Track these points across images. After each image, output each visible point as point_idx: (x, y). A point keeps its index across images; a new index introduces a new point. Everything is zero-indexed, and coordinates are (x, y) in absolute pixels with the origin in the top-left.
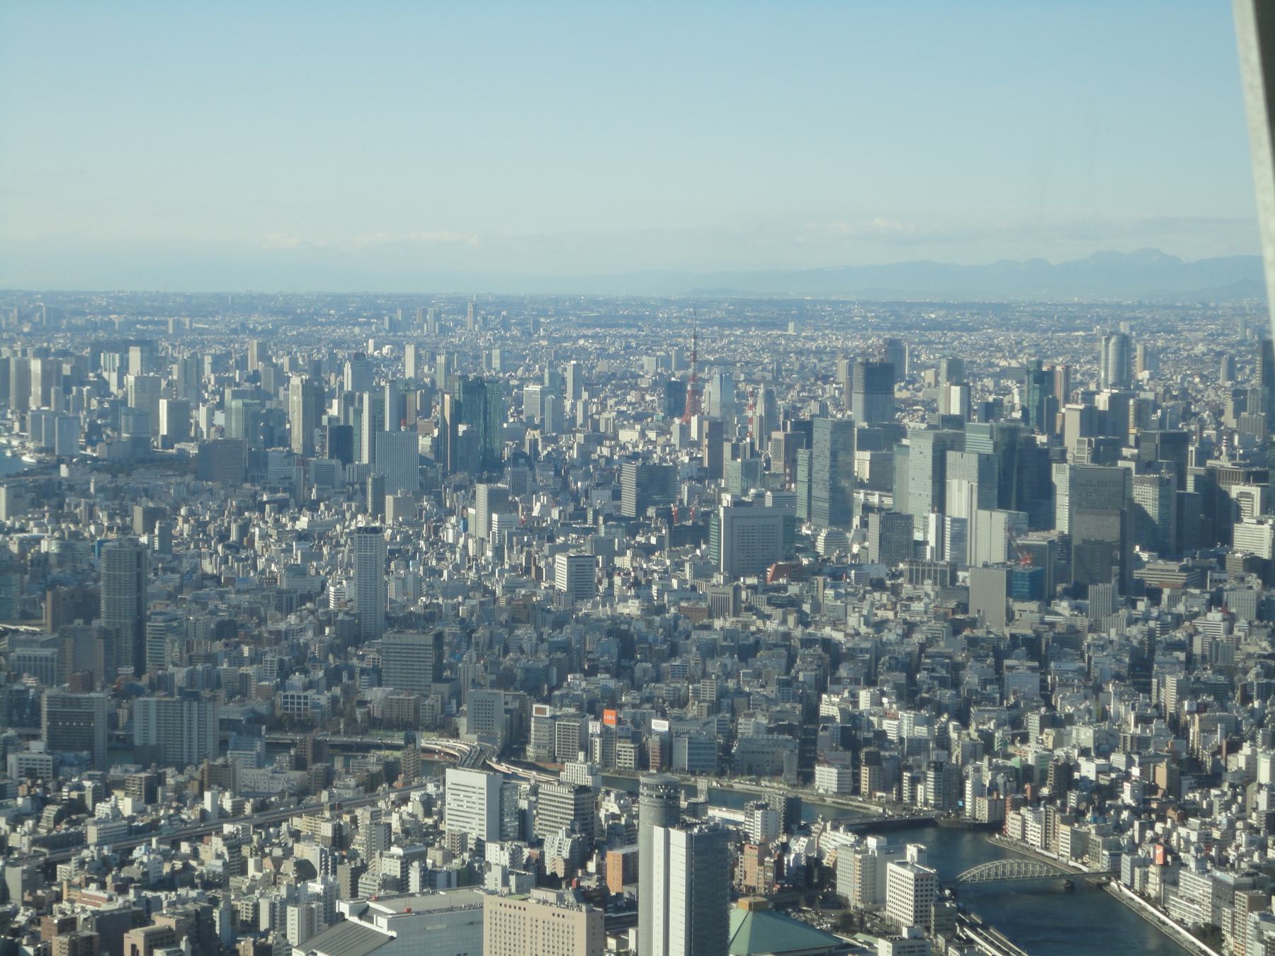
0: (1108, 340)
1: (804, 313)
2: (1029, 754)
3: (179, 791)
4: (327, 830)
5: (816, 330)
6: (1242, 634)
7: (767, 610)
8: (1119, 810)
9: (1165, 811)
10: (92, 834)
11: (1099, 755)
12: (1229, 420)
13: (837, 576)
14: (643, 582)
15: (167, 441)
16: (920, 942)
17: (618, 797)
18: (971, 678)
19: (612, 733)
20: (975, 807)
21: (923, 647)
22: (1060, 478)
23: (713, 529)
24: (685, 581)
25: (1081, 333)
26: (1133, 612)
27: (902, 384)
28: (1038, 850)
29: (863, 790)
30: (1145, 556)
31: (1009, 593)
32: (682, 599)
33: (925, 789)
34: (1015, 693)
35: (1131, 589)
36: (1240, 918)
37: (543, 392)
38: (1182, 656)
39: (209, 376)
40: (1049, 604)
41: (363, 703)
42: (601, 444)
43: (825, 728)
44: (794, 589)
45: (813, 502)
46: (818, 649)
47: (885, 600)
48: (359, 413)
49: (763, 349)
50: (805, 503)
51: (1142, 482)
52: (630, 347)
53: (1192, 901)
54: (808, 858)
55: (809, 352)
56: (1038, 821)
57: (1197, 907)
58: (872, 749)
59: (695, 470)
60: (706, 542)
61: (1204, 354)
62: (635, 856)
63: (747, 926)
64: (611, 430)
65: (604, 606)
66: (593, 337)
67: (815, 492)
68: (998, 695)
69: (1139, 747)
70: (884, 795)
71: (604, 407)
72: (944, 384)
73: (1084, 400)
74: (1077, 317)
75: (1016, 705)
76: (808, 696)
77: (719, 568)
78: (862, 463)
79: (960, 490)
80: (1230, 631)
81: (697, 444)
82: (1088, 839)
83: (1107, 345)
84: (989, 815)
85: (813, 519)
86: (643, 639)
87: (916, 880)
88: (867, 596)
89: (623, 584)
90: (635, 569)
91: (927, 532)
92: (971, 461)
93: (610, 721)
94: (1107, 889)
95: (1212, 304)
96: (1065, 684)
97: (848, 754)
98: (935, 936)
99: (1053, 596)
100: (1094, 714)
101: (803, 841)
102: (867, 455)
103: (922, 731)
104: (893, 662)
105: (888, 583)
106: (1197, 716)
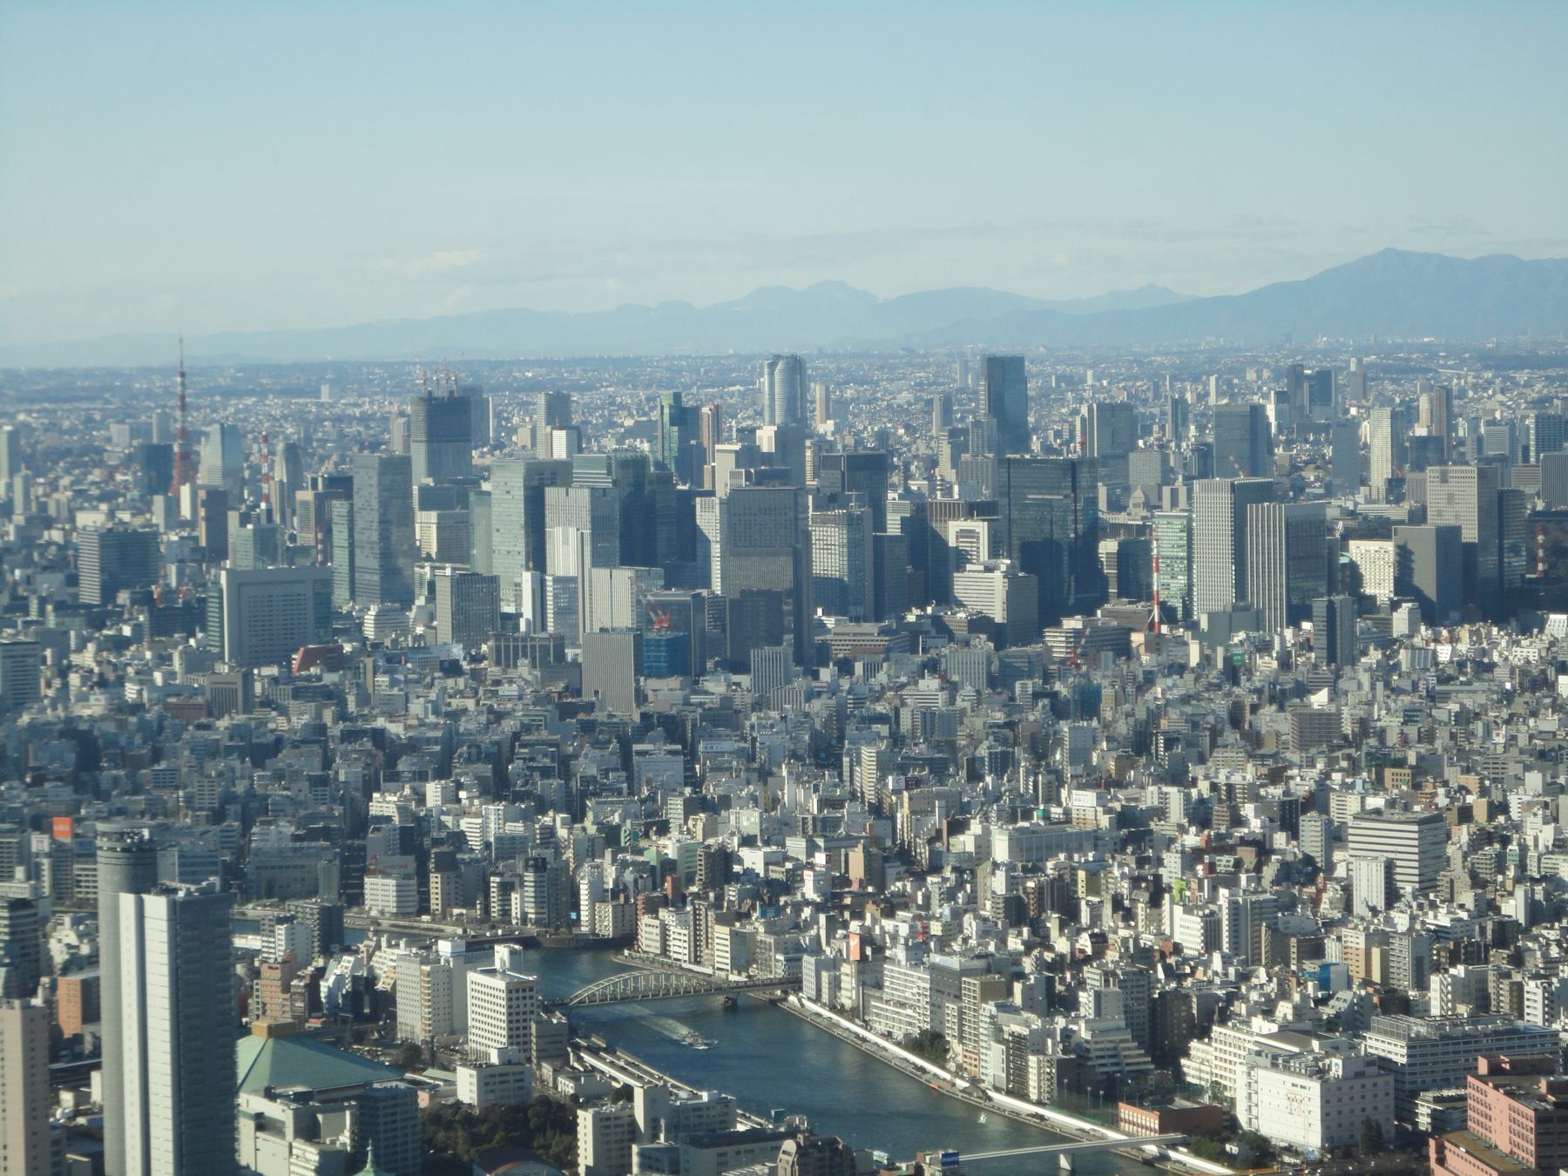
0: (772, 366)
1: (345, 377)
2: (669, 846)
5: (360, 396)
6: (967, 705)
7: (293, 704)
8: (798, 908)
9: (863, 906)
11: (767, 843)
12: (945, 470)
13: (392, 661)
14: (111, 677)
16: (517, 1069)
17: (76, 922)
18: (586, 766)
19: (65, 851)
20: (594, 918)
21: (516, 736)
22: (709, 519)
23: (212, 606)
24: (173, 674)
25: (738, 387)
26: (814, 684)
27: (485, 450)
28: (685, 966)
29: (433, 907)
30: (830, 622)
31: (639, 670)
32: (169, 696)
33: (522, 897)
34: (649, 783)
35: (811, 656)
36: (970, 1015)
38: (884, 730)
40: (697, 682)
42: (49, 527)
43: (378, 830)
44: (330, 678)
45: (357, 575)
46: (368, 744)
47: (462, 687)
49: (285, 417)
50: (346, 578)
51: (824, 522)
52: (94, 421)
53: (903, 1005)
54: (356, 980)
55: (351, 419)
56: (683, 924)
57: (909, 1012)
58: (445, 849)
59: (186, 551)
60: (202, 630)
61: (910, 404)
62: (98, 979)
63: (266, 1059)
64: (65, 514)
65: (55, 708)
66: (38, 411)
67: (360, 561)
68: (625, 785)
69: (824, 829)
70: (464, 911)
71: (54, 486)
72: (544, 429)
73: (740, 440)
74: (733, 370)
75: (652, 798)
76: (352, 799)
77: (222, 658)
78: (426, 528)
79: (566, 542)
80: (952, 701)
81: (192, 524)
82: (755, 940)
83: (771, 374)
84: (615, 927)
85: (358, 598)
86: (112, 742)
87: (509, 991)
88: (436, 682)
89: (83, 683)
90: (99, 663)
93: (63, 833)
94: (785, 1006)
95: (922, 352)
96: (717, 769)
97: (410, 861)
98: (539, 1067)
99: (703, 672)
100: (761, 801)
101: (348, 961)
102: (432, 516)
103: (517, 828)
104: (474, 751)
105: (465, 666)
106: (906, 794)
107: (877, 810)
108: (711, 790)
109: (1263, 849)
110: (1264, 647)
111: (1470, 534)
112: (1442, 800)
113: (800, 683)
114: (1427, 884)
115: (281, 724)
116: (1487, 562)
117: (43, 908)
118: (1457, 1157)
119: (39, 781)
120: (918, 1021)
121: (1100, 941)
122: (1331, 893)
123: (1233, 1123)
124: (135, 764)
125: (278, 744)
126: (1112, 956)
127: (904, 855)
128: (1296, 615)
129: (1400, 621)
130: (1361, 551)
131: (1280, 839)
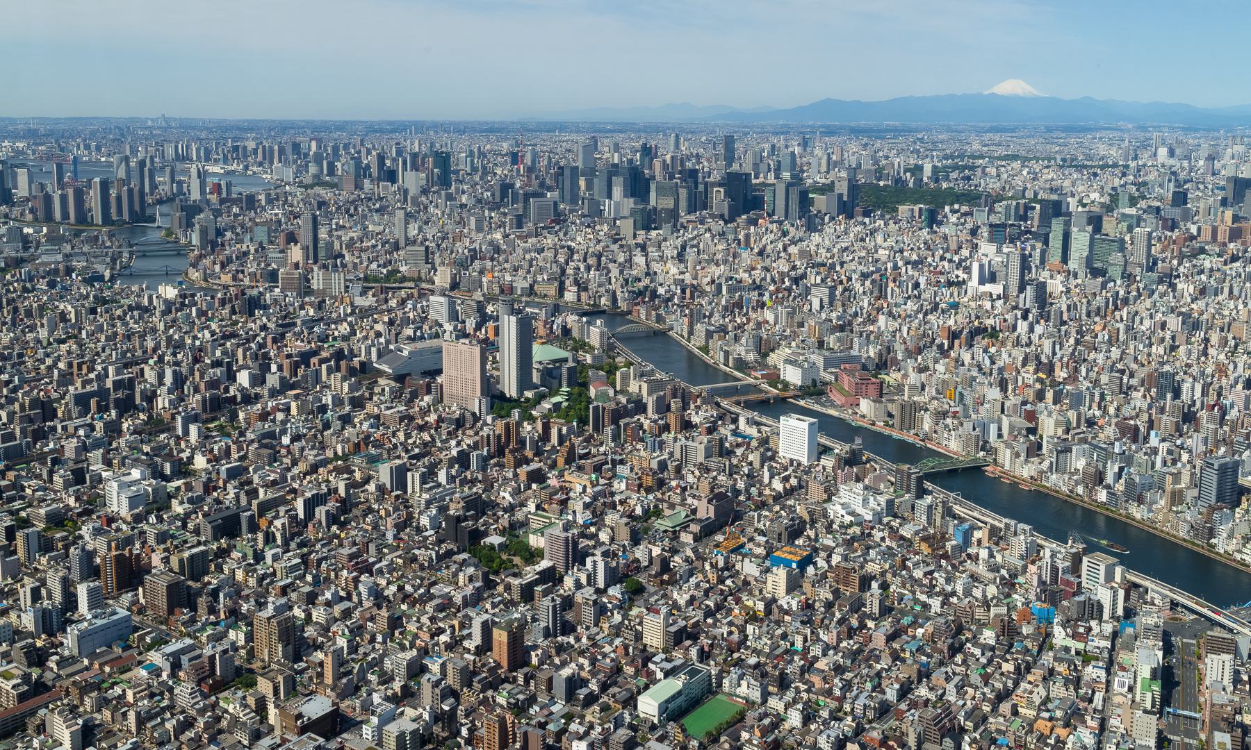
1: (563, 127)
4: (386, 319)
10: (299, 322)
22: (653, 186)
37: (466, 157)
48: (398, 165)
78: (582, 183)
112: (835, 278)
114: (831, 304)
123: (779, 376)
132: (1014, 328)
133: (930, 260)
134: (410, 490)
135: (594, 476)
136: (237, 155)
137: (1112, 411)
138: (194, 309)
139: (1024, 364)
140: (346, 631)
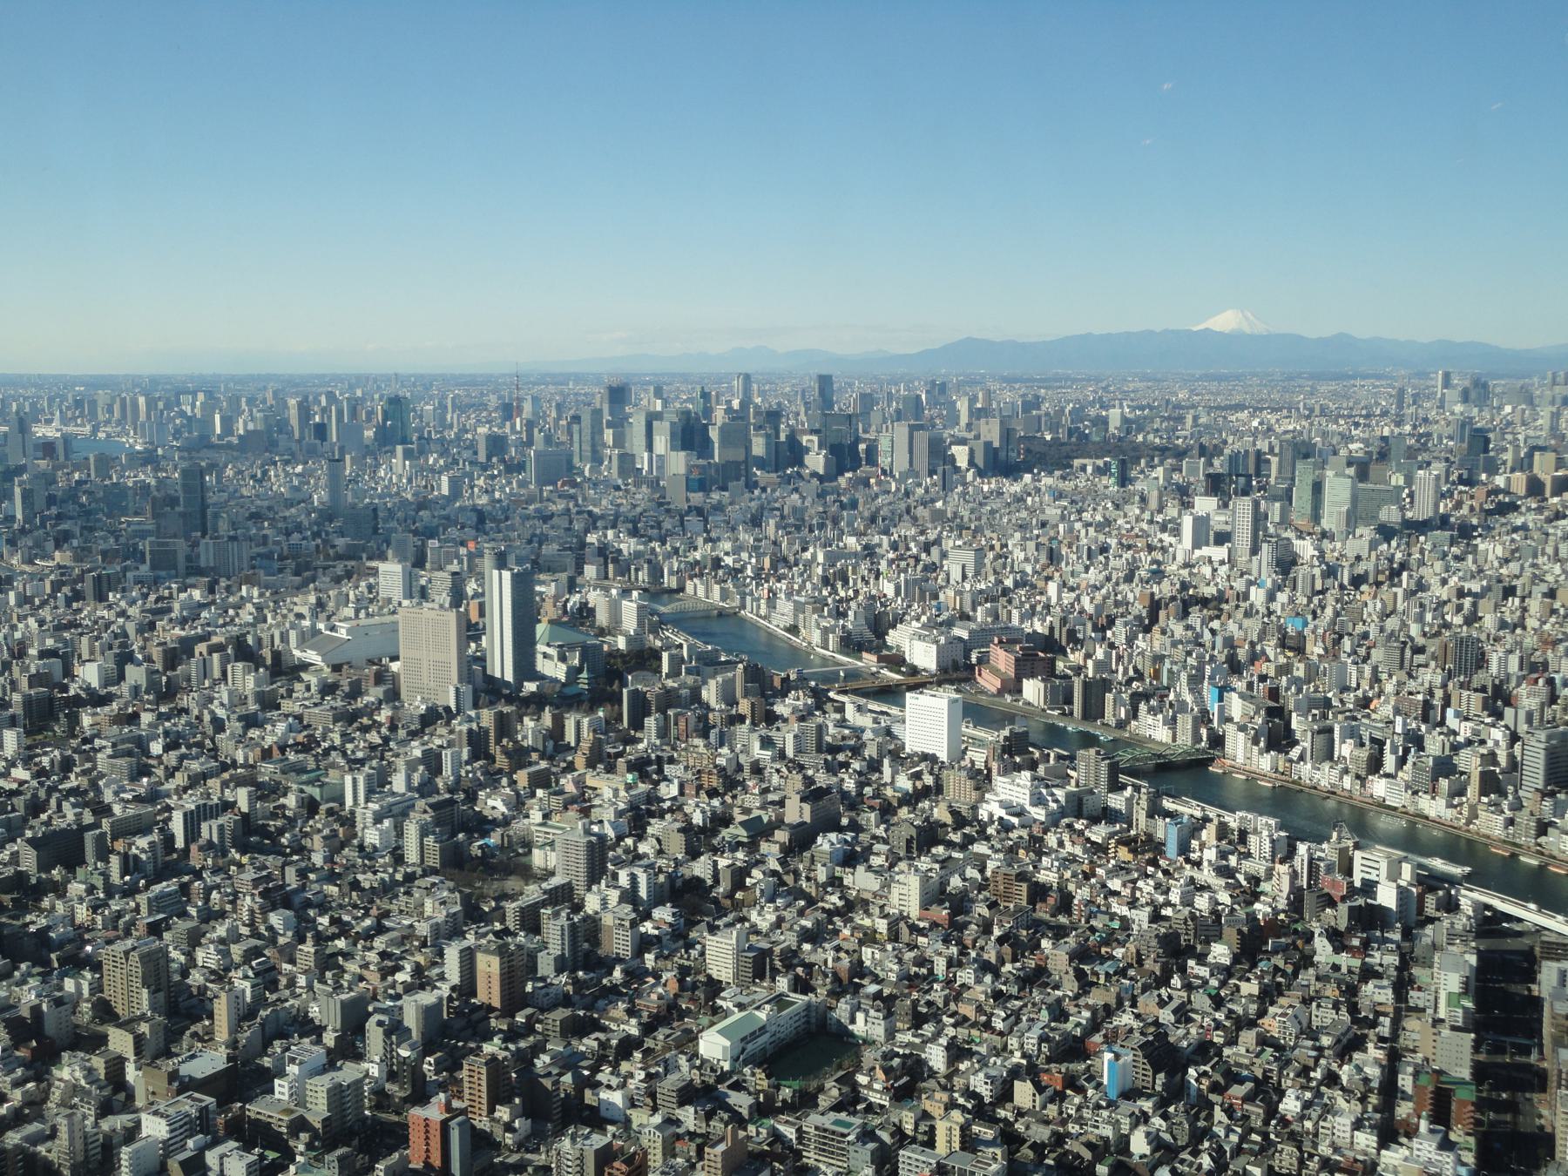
1: (579, 378)
2: (698, 555)
3: (228, 588)
4: (312, 599)
10: (176, 606)
12: (802, 417)
13: (595, 485)
15: (220, 437)
18: (667, 525)
20: (670, 581)
22: (714, 434)
31: (688, 489)
35: (751, 485)
39: (244, 406)
41: (333, 547)
44: (572, 491)
48: (330, 417)
78: (608, 436)
91: (643, 463)
92: (666, 425)
103: (641, 547)
107: (775, 543)
108: (713, 535)
109: (917, 559)
110: (920, 485)
111: (996, 444)
113: (747, 495)
114: (977, 573)
115: (553, 508)
116: (1002, 455)
117: (464, 575)
118: (985, 672)
119: (463, 527)
120: (789, 621)
121: (856, 592)
122: (942, 576)
124: (500, 521)
125: (552, 515)
126: (861, 598)
127: (785, 560)
128: (931, 473)
129: (970, 476)
130: (955, 449)
131: (923, 556)
132: (1246, 596)
133: (1120, 522)
134: (349, 802)
135: (630, 777)
136: (82, 412)
137: (1389, 688)
138: (12, 595)
139: (1262, 635)
140: (250, 973)
